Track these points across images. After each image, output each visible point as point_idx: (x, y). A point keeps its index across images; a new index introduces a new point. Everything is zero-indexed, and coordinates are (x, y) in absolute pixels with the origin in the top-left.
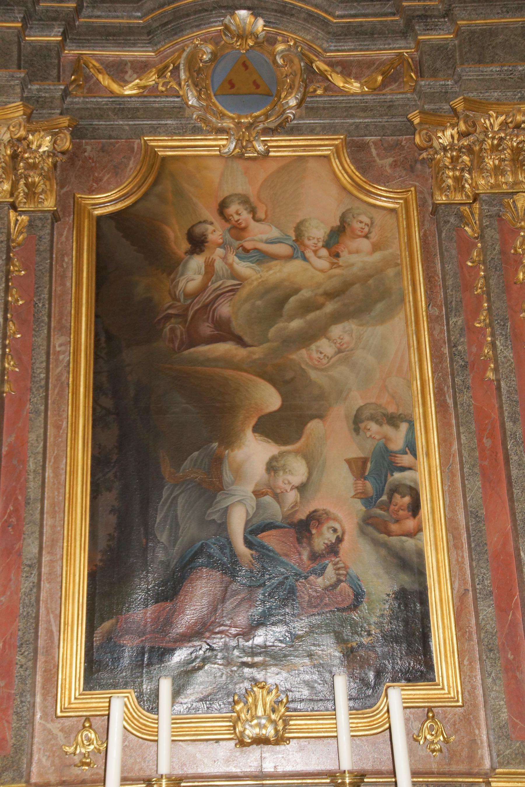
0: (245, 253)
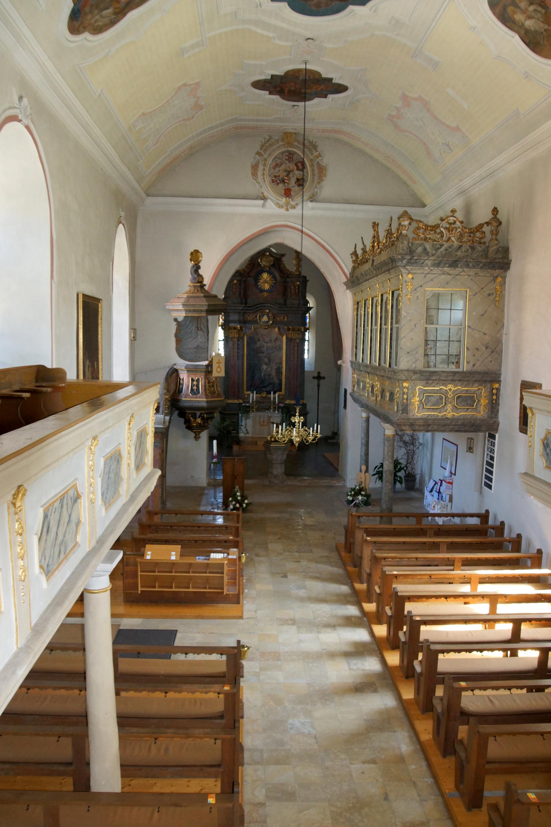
0: (265, 342)
